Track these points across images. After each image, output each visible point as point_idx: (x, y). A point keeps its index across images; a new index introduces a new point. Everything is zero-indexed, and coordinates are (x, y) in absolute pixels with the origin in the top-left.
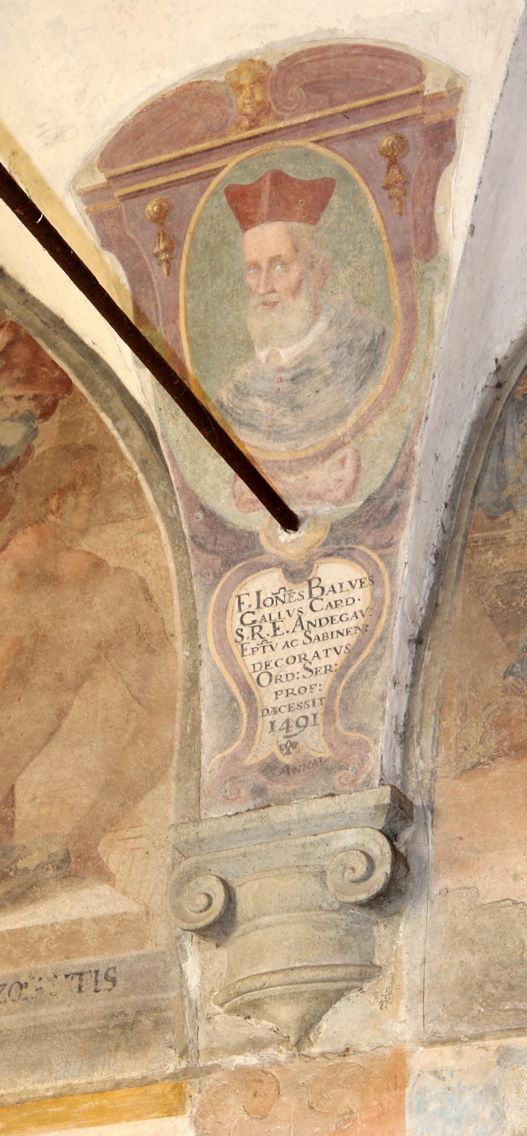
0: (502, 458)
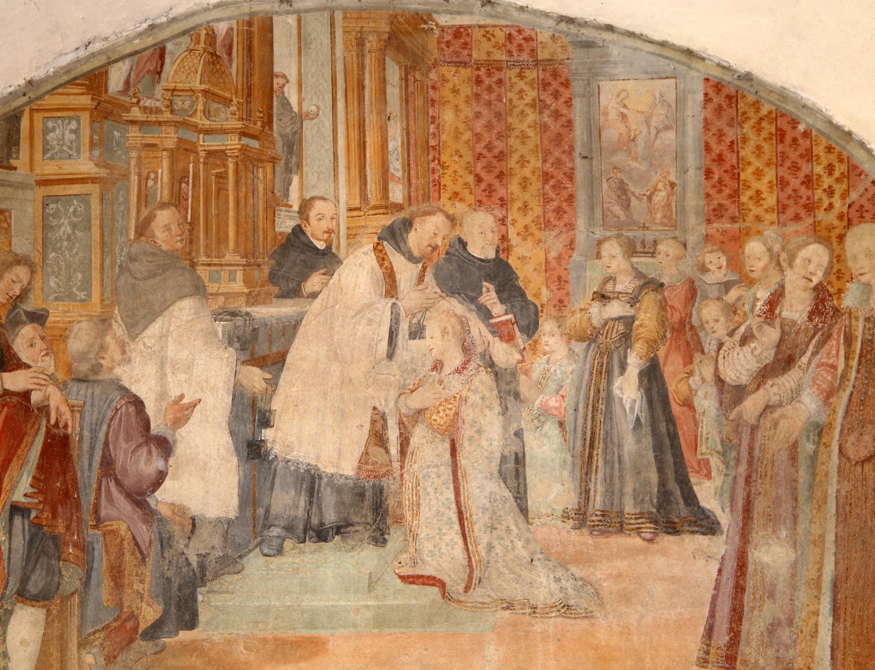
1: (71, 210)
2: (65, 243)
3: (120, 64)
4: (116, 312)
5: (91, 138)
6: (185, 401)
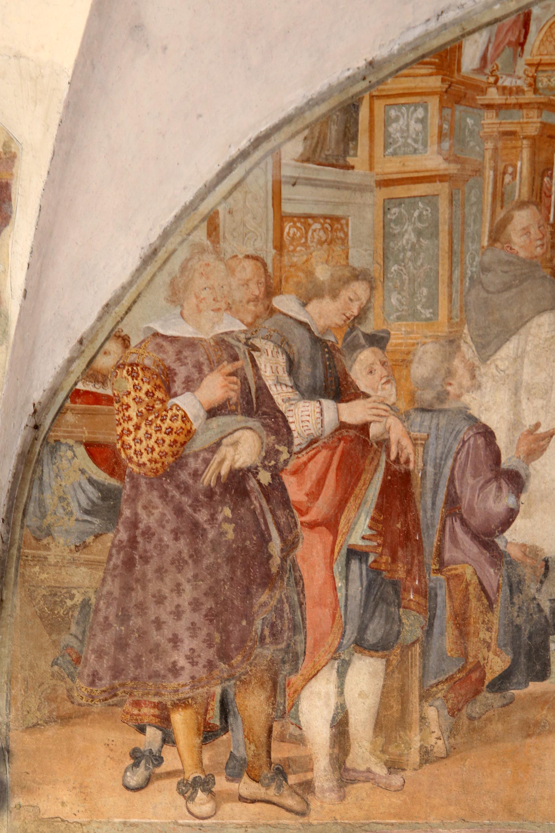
0: (42, 492)
1: (416, 214)
2: (409, 254)
3: (476, 36)
4: (466, 331)
5: (440, 128)
6: (541, 430)
